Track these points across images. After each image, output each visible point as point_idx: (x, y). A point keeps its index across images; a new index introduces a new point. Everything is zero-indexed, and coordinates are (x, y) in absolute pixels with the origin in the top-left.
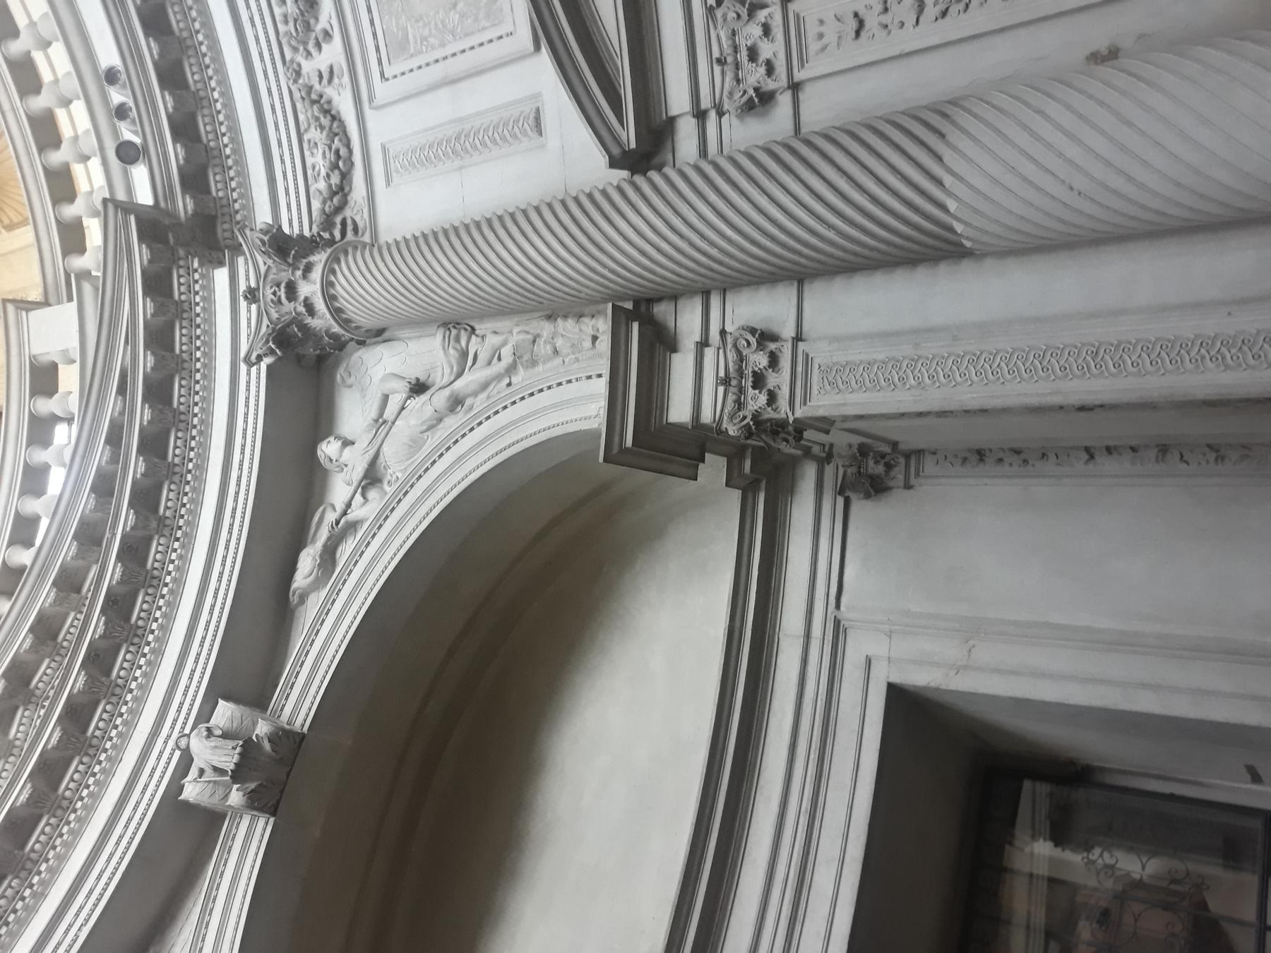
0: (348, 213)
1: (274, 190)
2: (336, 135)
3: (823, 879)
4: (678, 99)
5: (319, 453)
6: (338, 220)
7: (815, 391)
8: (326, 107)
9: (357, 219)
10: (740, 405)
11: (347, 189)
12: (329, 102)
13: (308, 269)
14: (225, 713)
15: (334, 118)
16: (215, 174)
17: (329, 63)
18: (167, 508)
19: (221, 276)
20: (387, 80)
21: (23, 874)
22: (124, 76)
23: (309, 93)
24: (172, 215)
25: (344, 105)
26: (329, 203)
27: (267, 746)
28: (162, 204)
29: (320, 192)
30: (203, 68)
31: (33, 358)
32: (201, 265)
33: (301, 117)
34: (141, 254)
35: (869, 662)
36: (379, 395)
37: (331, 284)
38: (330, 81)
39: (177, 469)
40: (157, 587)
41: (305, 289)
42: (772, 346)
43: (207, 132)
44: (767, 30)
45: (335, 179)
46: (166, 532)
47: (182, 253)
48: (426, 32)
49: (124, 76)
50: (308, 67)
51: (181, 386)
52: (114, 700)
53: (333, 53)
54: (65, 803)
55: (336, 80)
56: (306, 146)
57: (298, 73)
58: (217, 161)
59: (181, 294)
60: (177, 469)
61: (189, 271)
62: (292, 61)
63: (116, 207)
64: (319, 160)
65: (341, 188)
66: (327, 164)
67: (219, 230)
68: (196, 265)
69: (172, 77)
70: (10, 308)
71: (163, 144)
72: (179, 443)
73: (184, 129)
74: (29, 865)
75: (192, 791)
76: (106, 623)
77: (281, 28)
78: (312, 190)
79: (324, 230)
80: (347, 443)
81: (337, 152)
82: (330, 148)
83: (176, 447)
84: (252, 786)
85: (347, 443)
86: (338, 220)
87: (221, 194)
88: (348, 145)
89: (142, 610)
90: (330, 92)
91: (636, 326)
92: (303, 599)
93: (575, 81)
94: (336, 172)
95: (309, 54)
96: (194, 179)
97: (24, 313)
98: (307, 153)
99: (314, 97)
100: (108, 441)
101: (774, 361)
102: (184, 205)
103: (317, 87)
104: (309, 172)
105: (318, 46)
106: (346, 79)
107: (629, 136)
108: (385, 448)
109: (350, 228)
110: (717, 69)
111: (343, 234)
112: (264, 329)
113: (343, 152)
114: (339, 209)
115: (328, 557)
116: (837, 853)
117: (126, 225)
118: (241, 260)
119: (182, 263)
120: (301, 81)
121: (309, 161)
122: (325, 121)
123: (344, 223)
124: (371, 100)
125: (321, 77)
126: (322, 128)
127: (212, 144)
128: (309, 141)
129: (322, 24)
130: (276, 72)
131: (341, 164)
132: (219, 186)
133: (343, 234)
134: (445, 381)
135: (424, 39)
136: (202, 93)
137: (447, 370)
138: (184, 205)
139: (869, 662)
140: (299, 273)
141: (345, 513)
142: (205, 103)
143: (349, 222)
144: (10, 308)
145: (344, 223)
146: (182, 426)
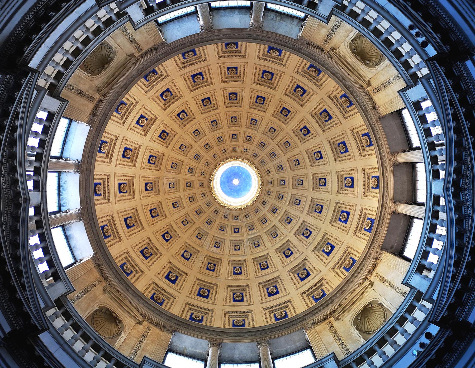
22: (414, 26)
28: (440, 52)
31: (412, 102)
49: (414, 26)
51: (469, 98)
59: (458, 73)
61: (457, 66)
68: (459, 63)
70: (400, 92)
73: (436, 28)
96: (446, 39)
102: (446, 48)
136: (438, 16)
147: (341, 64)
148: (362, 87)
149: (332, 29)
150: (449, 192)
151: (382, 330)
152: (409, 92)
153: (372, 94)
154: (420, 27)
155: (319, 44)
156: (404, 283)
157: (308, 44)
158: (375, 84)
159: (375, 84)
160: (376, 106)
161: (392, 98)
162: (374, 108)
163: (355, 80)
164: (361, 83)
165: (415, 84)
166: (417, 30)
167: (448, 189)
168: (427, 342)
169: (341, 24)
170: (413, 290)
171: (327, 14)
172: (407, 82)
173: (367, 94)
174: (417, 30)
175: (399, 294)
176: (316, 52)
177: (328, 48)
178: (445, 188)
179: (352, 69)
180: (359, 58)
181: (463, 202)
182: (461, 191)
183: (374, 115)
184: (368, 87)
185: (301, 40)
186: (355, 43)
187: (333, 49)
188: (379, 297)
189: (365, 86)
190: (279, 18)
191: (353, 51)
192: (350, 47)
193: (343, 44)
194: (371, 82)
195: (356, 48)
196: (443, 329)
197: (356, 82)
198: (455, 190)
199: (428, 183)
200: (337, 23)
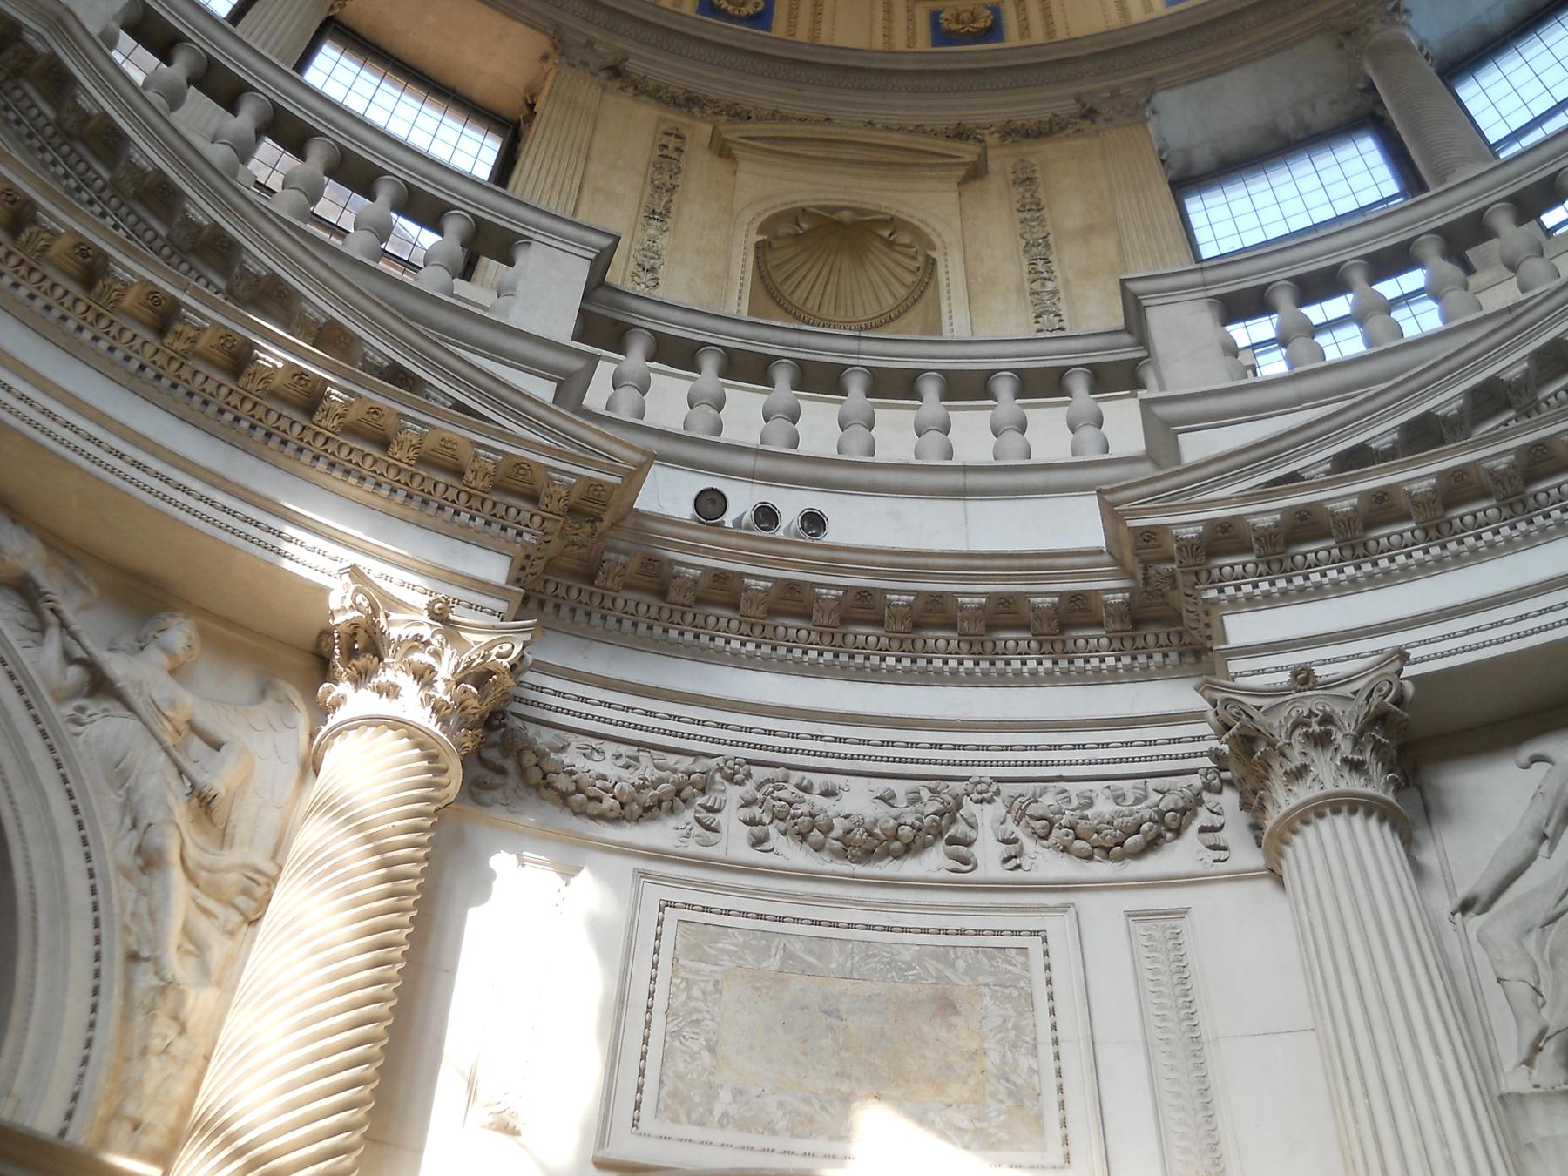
0: (513, 780)
6: (509, 764)
9: (497, 794)
11: (545, 793)
12: (672, 810)
15: (647, 809)
17: (724, 829)
19: (495, 568)
20: (661, 909)
22: (808, 539)
25: (660, 834)
26: (534, 760)
29: (562, 749)
31: (528, 242)
33: (671, 759)
38: (698, 820)
45: (563, 782)
48: (696, 992)
50: (734, 794)
53: (734, 842)
55: (698, 830)
56: (632, 750)
57: (730, 779)
62: (748, 775)
64: (605, 767)
66: (585, 778)
69: (792, 601)
71: (707, 553)
77: (796, 776)
78: (570, 737)
79: (504, 736)
86: (509, 764)
88: (601, 817)
90: (689, 815)
94: (572, 787)
95: (747, 804)
97: (592, 256)
98: (624, 749)
99: (688, 791)
100: (332, 323)
103: (700, 800)
104: (594, 742)
105: (751, 822)
106: (692, 848)
108: (132, 723)
113: (593, 808)
114: (523, 772)
117: (612, 471)
118: (501, 606)
120: (718, 776)
121: (610, 748)
122: (648, 795)
123: (501, 771)
125: (710, 810)
126: (639, 788)
128: (636, 759)
129: (777, 840)
130: (743, 745)
131: (580, 797)
135: (690, 985)
141: (64, 625)
143: (498, 779)
144: (605, 242)
145: (501, 771)
147: (897, 139)
148: (740, 115)
149: (1047, 246)
152: (579, 273)
153: (675, 118)
154: (780, 548)
155: (1047, 150)
157: (1090, 114)
158: (699, 168)
159: (699, 168)
160: (614, 85)
161: (594, 169)
162: (616, 71)
163: (785, 118)
164: (754, 129)
166: (780, 533)
169: (1034, 293)
171: (1158, 319)
173: (689, 102)
174: (780, 533)
176: (1032, 107)
177: (1001, 161)
179: (830, 150)
180: (846, 216)
183: (590, 44)
184: (715, 133)
185: (1136, 110)
186: (914, 258)
187: (976, 173)
189: (733, 132)
190: (1287, 124)
191: (892, 222)
192: (916, 232)
193: (957, 223)
194: (719, 164)
195: (890, 244)
197: (776, 116)
200: (1050, 286)
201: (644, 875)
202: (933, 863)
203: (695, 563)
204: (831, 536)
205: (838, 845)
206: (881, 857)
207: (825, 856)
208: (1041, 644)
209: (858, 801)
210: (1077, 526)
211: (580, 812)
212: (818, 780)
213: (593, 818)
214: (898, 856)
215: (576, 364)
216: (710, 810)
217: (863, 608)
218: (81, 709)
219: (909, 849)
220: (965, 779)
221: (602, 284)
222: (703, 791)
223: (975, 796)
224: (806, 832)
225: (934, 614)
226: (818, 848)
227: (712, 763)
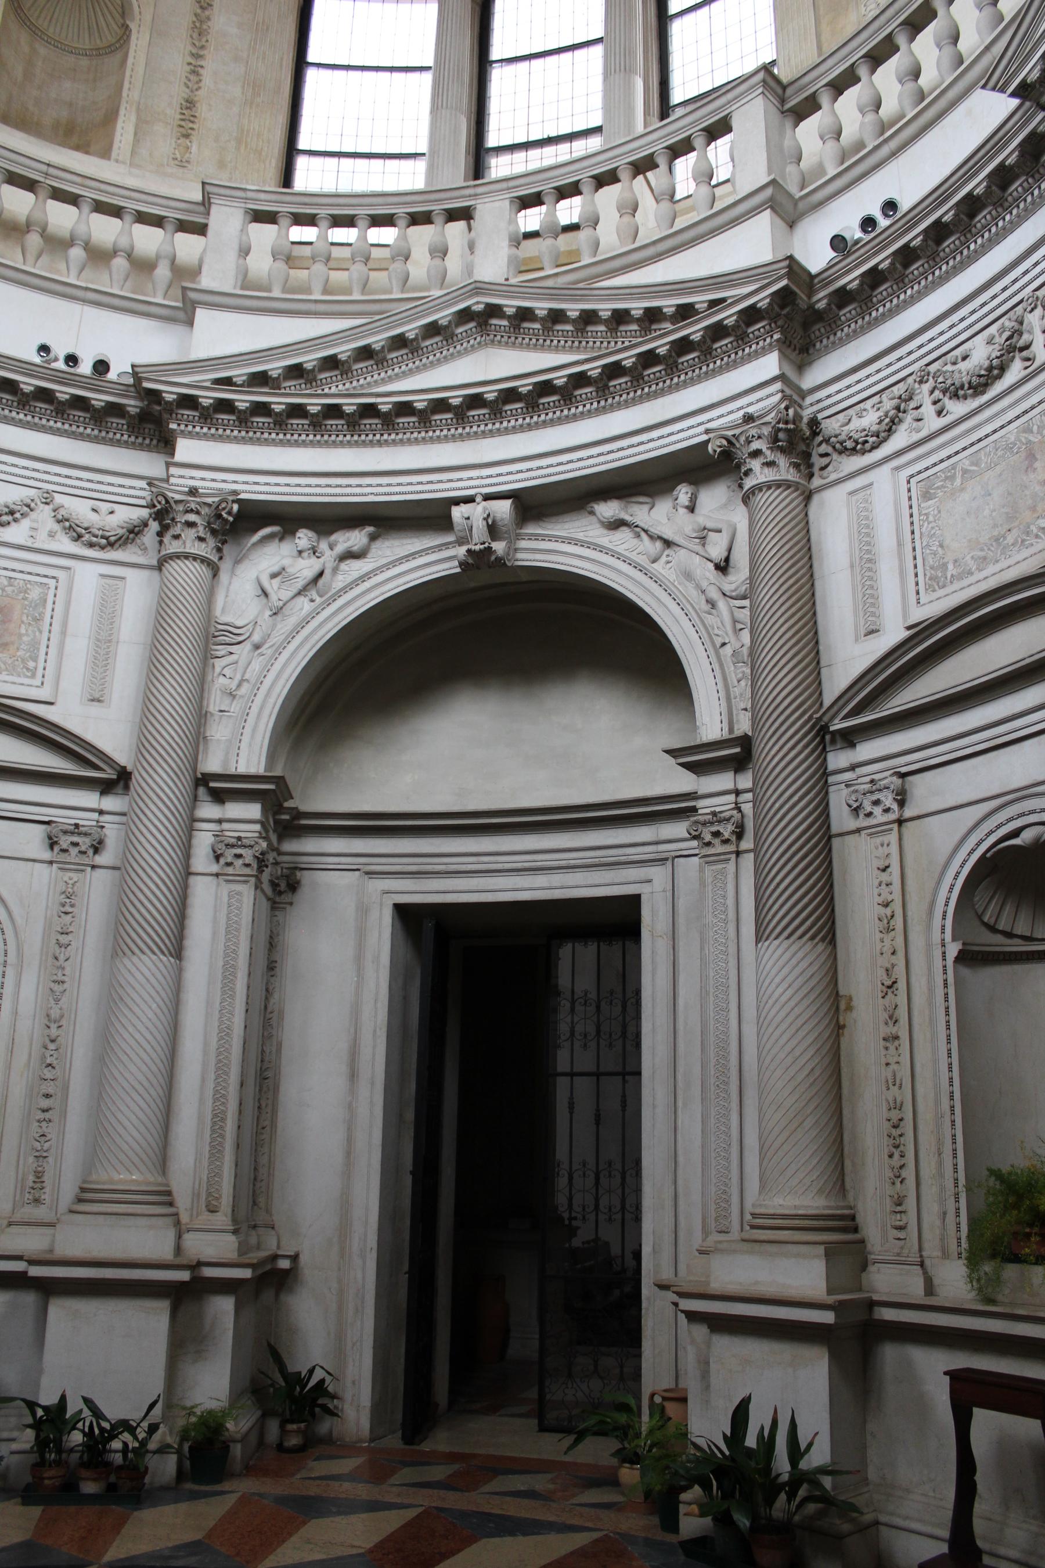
0: (835, 456)
1: (847, 374)
2: (878, 437)
3: (541, 880)
4: (867, 750)
5: (679, 487)
7: (714, 867)
8: (897, 420)
9: (830, 468)
10: (704, 824)
12: (901, 421)
13: (770, 464)
14: (503, 508)
16: (855, 309)
18: (615, 386)
19: (769, 365)
21: (385, 427)
23: (906, 401)
24: (811, 290)
25: (899, 439)
27: (493, 558)
28: (816, 281)
30: (924, 275)
32: (778, 340)
33: (895, 389)
34: (762, 299)
35: (650, 881)
36: (719, 526)
37: (760, 490)
39: (641, 382)
40: (566, 405)
41: (755, 464)
42: (734, 838)
43: (881, 293)
44: (887, 810)
46: (600, 393)
47: (779, 323)
48: (931, 519)
50: (926, 388)
51: (693, 359)
52: (492, 416)
54: (428, 424)
55: (915, 424)
56: (876, 399)
57: (921, 382)
58: (864, 308)
59: (753, 333)
60: (641, 382)
61: (770, 333)
63: (789, 266)
64: (869, 420)
65: (846, 449)
67: (817, 327)
68: (776, 336)
69: (907, 256)
71: (857, 266)
72: (658, 374)
73: (874, 278)
74: (391, 427)
75: (458, 513)
76: (529, 391)
80: (691, 509)
81: (866, 442)
82: (867, 436)
83: (654, 373)
84: (470, 561)
85: (691, 509)
86: (830, 450)
87: (843, 318)
88: (874, 448)
89: (549, 403)
90: (909, 418)
91: (738, 750)
92: (592, 513)
93: (864, 681)
94: (854, 444)
96: (843, 297)
97: (760, 90)
101: (726, 841)
102: (821, 299)
106: (916, 437)
107: (837, 725)
108: (683, 551)
109: (824, 461)
110: (868, 779)
111: (822, 456)
112: (730, 433)
113: (868, 446)
115: (617, 524)
116: (555, 884)
119: (773, 325)
122: (883, 426)
123: (827, 455)
124: (897, 469)
125: (917, 408)
127: (875, 300)
132: (848, 315)
133: (822, 456)
134: (727, 588)
136: (906, 280)
137: (733, 586)
138: (821, 299)
139: (650, 881)
140: (770, 456)
142: (901, 285)
145: (827, 455)
146: (669, 371)
150: (470, 296)
151: (52, 171)
156: (208, 188)
165: (789, 110)
167: (477, 294)
168: (85, 368)
170: (201, 209)
172: (797, 85)
175: (184, 93)
178: (478, 285)
181: (453, 335)
182: (480, 325)
188: (148, 17)
196: (132, 389)
198: (479, 314)
199: (504, 185)
201: (897, 469)
202: (1016, 371)
203: (851, 279)
204: (905, 204)
205: (970, 391)
206: (992, 383)
207: (969, 401)
208: (1033, 176)
209: (981, 353)
210: (989, 111)
211: (863, 452)
212: (958, 352)
213: (870, 451)
214: (999, 377)
215: (769, 192)
216: (917, 408)
217: (938, 232)
218: (668, 556)
219: (1003, 369)
220: (1021, 301)
221: (784, 88)
222: (911, 399)
223: (1029, 309)
224: (956, 393)
225: (971, 205)
226: (965, 397)
227: (910, 380)
